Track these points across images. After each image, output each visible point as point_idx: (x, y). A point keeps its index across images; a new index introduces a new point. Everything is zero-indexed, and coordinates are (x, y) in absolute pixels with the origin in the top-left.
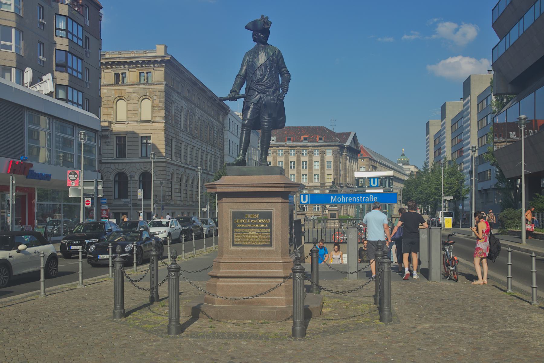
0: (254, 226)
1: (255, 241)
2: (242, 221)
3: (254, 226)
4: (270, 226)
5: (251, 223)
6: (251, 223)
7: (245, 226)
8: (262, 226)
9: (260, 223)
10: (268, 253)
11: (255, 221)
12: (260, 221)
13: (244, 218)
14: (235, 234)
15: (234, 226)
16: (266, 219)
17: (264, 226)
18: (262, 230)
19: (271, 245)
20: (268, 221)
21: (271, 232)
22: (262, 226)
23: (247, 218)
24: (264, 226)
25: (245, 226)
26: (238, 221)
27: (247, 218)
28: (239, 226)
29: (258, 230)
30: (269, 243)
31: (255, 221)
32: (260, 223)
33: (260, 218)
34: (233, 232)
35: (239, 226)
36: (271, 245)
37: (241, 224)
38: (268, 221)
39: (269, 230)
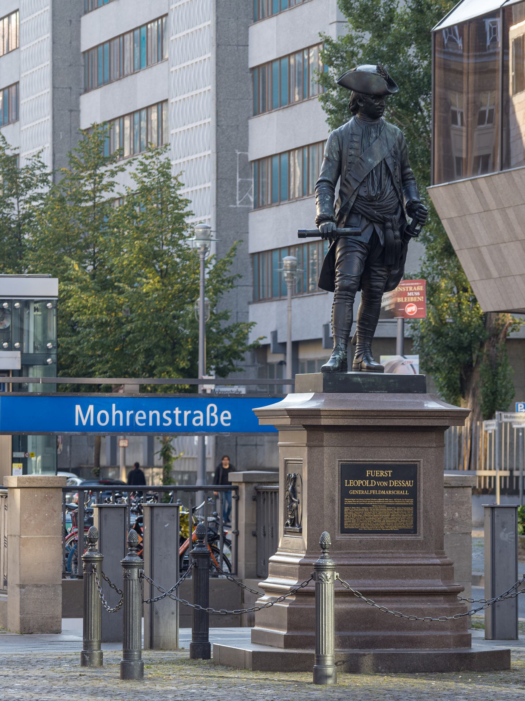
0: (383, 492)
1: (384, 522)
2: (359, 482)
3: (383, 492)
4: (413, 493)
5: (377, 488)
6: (377, 488)
7: (366, 493)
8: (398, 492)
9: (394, 488)
10: (408, 545)
11: (385, 484)
12: (395, 483)
13: (364, 478)
14: (346, 509)
15: (345, 493)
16: (406, 479)
17: (402, 493)
18: (398, 502)
19: (414, 531)
20: (409, 484)
21: (415, 506)
22: (398, 492)
23: (370, 478)
24: (402, 493)
25: (366, 493)
26: (352, 483)
27: (370, 478)
28: (353, 492)
29: (390, 502)
30: (410, 526)
31: (385, 484)
32: (394, 488)
33: (393, 478)
34: (343, 506)
35: (353, 492)
36: (414, 531)
37: (357, 488)
38: (409, 484)
39: (411, 501)
